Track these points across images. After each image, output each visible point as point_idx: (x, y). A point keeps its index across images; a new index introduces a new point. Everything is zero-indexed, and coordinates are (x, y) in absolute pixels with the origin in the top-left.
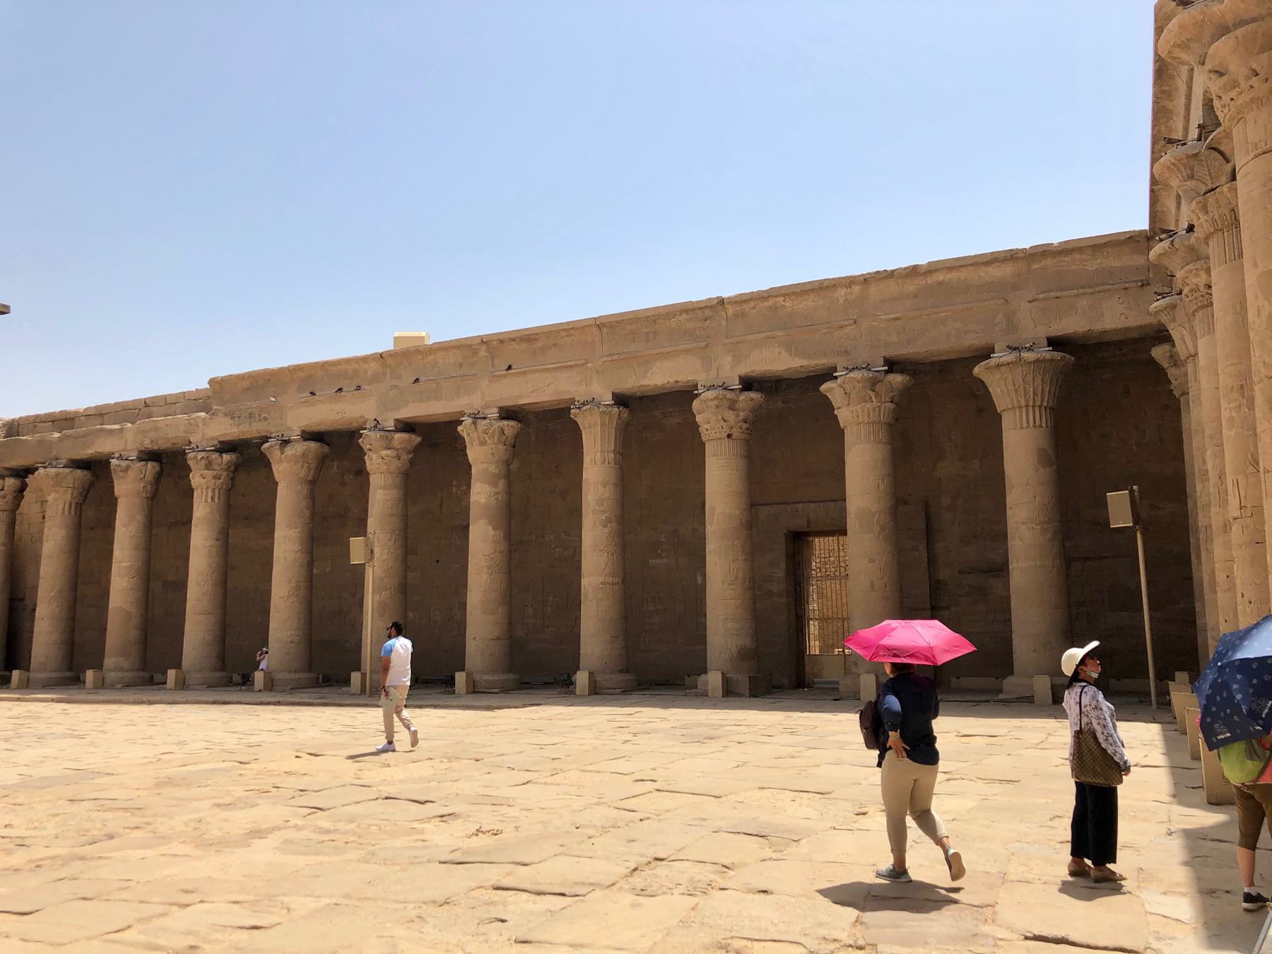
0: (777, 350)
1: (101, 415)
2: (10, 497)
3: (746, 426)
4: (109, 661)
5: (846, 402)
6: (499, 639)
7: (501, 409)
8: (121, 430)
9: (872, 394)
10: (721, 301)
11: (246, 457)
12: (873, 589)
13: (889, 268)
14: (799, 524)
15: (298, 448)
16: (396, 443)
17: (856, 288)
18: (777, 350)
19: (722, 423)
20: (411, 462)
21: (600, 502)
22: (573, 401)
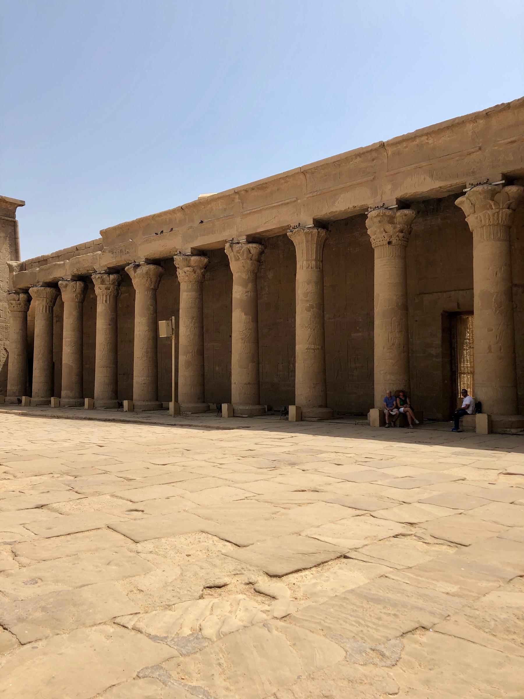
0: (422, 177)
1: (58, 256)
2: (22, 304)
3: (401, 235)
4: (63, 393)
5: (472, 211)
6: (249, 383)
7: (248, 236)
8: (64, 264)
9: (492, 203)
10: (382, 145)
11: (120, 275)
12: (490, 351)
13: (506, 101)
14: (452, 306)
15: (145, 268)
16: (192, 263)
17: (481, 122)
18: (422, 177)
19: (384, 234)
20: (203, 275)
21: (306, 294)
22: (288, 227)
